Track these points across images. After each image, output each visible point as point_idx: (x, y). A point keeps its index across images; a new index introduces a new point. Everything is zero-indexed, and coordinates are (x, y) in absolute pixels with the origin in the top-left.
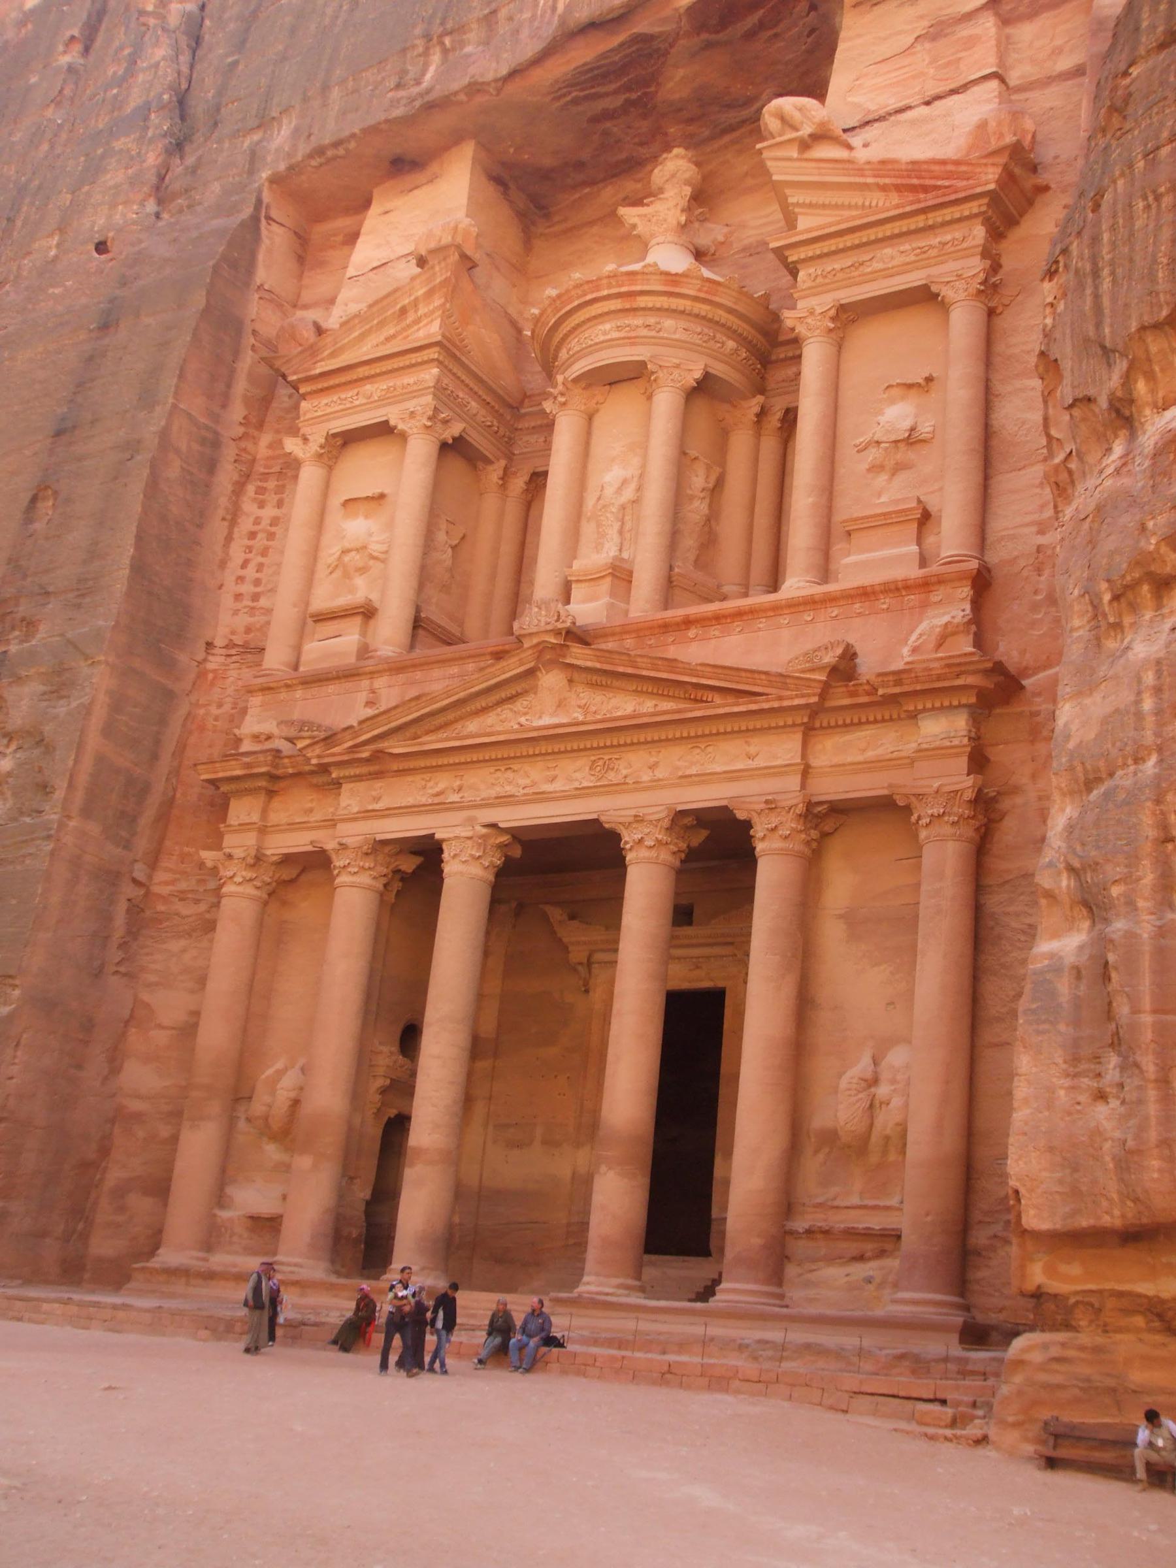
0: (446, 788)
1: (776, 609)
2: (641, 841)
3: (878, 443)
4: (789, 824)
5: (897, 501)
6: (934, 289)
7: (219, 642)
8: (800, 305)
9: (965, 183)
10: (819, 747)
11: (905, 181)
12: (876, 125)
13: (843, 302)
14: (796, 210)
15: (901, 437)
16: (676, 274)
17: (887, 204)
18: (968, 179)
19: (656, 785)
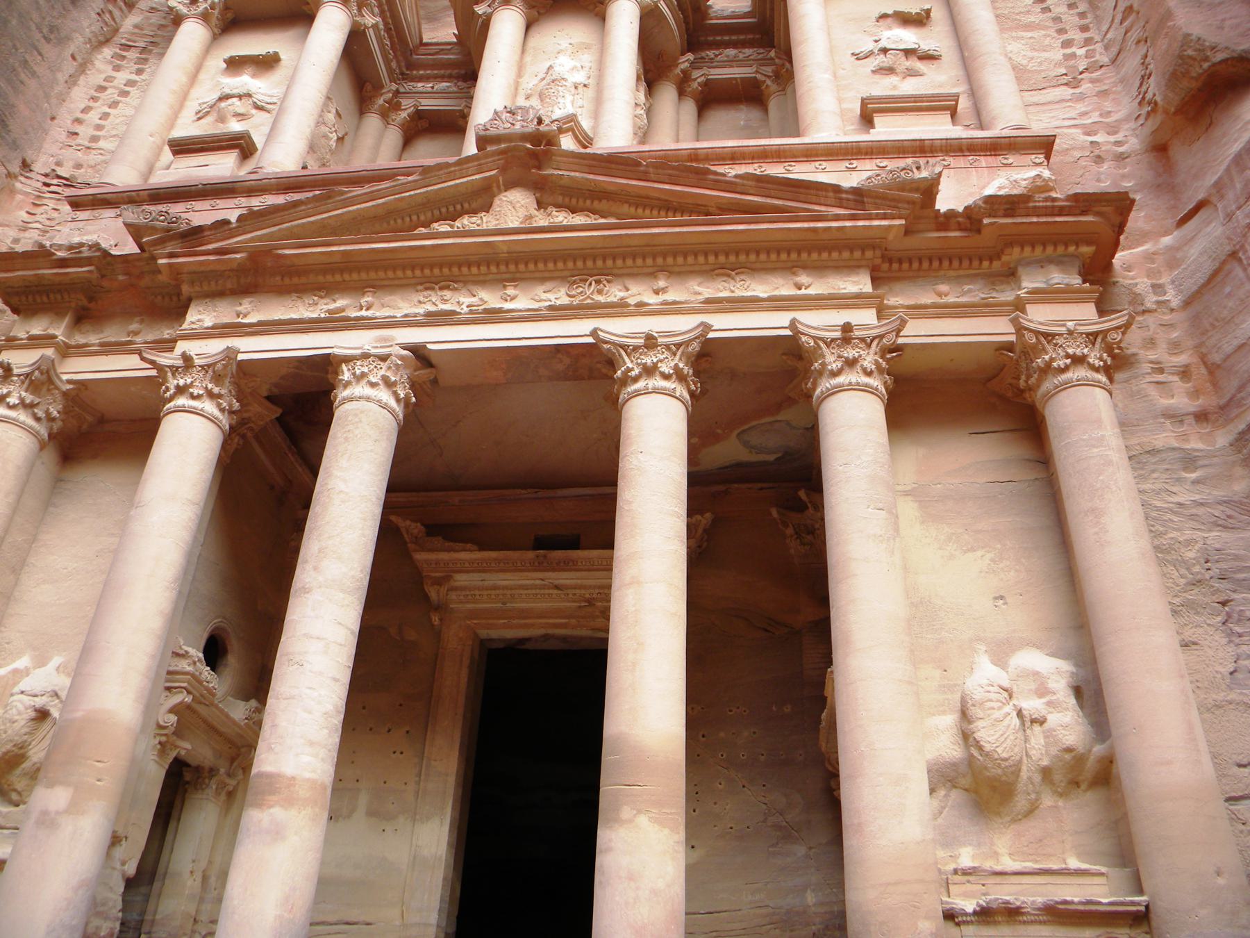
0: (347, 306)
2: (655, 366)
3: (885, 51)
4: (869, 359)
7: (40, 166)
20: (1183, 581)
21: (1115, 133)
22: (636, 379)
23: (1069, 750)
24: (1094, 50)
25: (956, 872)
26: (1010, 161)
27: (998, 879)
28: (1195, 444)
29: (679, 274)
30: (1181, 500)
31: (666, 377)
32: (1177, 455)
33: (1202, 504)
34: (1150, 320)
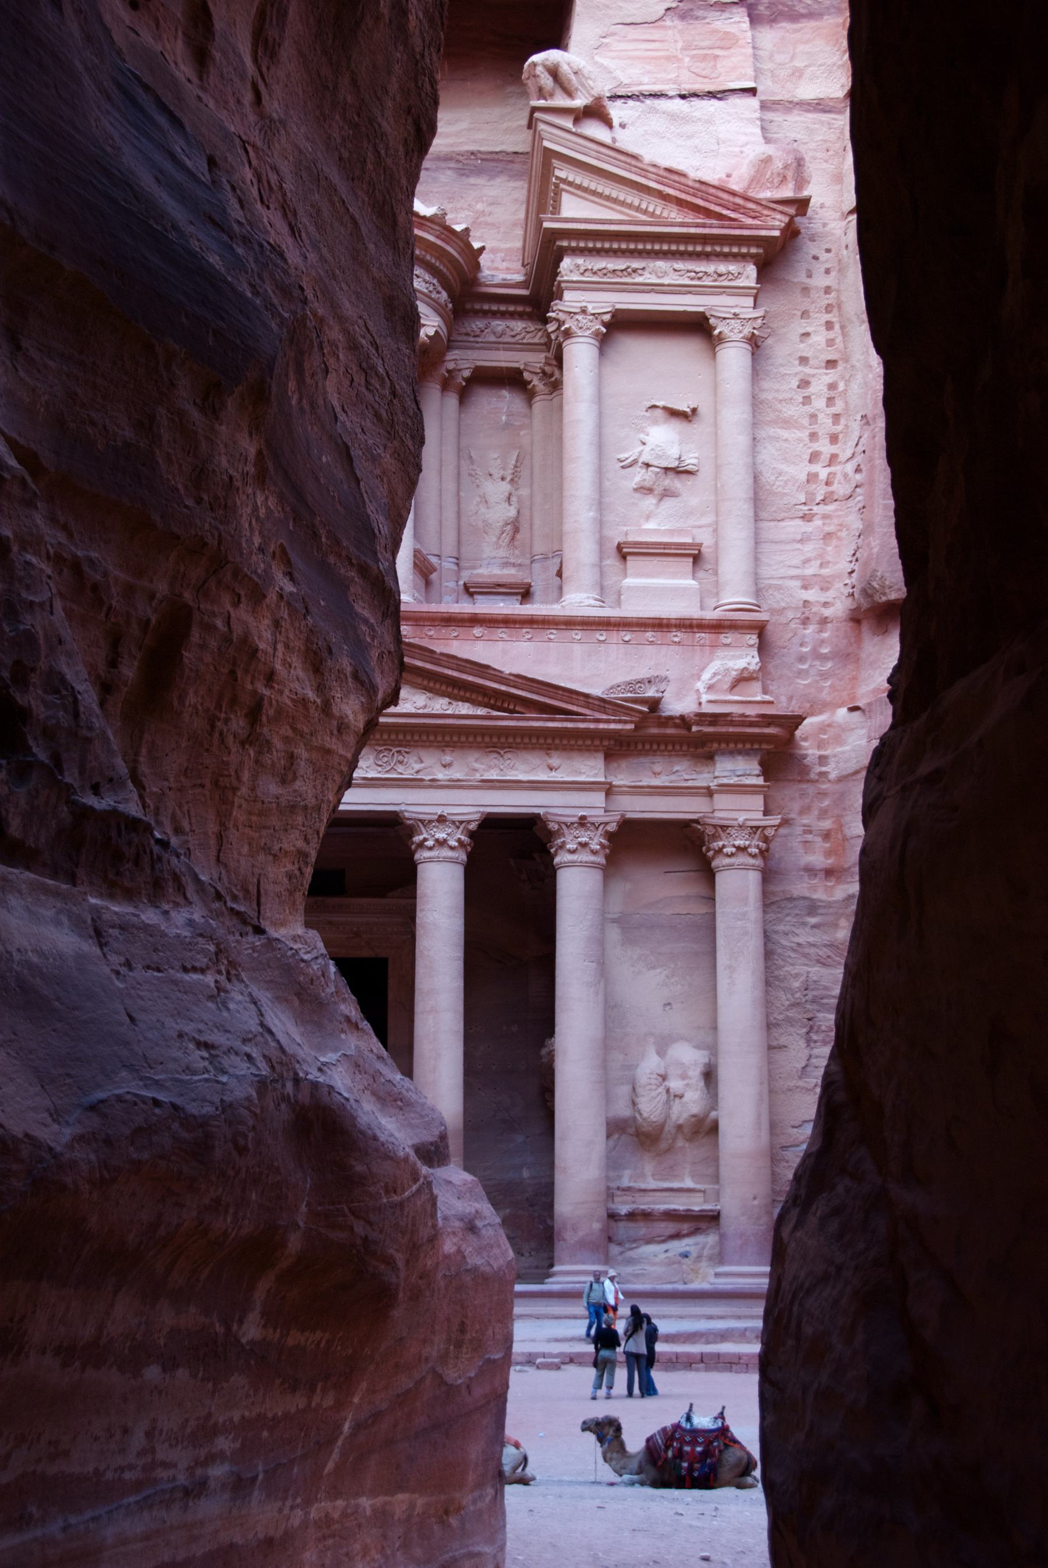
1: (569, 623)
2: (445, 841)
3: (648, 465)
5: (671, 532)
6: (712, 321)
8: (567, 295)
9: (749, 221)
10: (615, 765)
11: (689, 198)
12: (631, 103)
13: (618, 306)
14: (562, 186)
15: (672, 466)
16: (424, 218)
17: (665, 214)
18: (754, 218)
19: (455, 785)
20: (787, 1003)
21: (828, 589)
22: (431, 849)
23: (694, 1116)
24: (835, 474)
25: (618, 1188)
26: (728, 641)
27: (642, 1194)
28: (819, 895)
29: (462, 747)
30: (800, 940)
31: (452, 848)
32: (807, 903)
33: (814, 945)
34: (811, 789)
